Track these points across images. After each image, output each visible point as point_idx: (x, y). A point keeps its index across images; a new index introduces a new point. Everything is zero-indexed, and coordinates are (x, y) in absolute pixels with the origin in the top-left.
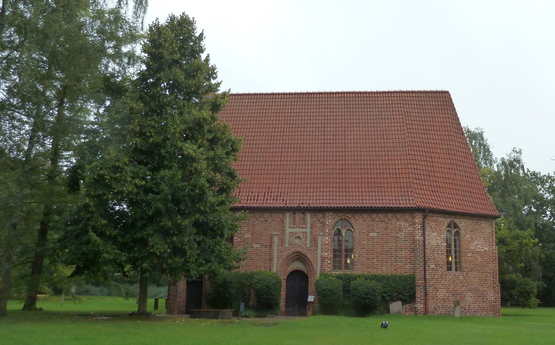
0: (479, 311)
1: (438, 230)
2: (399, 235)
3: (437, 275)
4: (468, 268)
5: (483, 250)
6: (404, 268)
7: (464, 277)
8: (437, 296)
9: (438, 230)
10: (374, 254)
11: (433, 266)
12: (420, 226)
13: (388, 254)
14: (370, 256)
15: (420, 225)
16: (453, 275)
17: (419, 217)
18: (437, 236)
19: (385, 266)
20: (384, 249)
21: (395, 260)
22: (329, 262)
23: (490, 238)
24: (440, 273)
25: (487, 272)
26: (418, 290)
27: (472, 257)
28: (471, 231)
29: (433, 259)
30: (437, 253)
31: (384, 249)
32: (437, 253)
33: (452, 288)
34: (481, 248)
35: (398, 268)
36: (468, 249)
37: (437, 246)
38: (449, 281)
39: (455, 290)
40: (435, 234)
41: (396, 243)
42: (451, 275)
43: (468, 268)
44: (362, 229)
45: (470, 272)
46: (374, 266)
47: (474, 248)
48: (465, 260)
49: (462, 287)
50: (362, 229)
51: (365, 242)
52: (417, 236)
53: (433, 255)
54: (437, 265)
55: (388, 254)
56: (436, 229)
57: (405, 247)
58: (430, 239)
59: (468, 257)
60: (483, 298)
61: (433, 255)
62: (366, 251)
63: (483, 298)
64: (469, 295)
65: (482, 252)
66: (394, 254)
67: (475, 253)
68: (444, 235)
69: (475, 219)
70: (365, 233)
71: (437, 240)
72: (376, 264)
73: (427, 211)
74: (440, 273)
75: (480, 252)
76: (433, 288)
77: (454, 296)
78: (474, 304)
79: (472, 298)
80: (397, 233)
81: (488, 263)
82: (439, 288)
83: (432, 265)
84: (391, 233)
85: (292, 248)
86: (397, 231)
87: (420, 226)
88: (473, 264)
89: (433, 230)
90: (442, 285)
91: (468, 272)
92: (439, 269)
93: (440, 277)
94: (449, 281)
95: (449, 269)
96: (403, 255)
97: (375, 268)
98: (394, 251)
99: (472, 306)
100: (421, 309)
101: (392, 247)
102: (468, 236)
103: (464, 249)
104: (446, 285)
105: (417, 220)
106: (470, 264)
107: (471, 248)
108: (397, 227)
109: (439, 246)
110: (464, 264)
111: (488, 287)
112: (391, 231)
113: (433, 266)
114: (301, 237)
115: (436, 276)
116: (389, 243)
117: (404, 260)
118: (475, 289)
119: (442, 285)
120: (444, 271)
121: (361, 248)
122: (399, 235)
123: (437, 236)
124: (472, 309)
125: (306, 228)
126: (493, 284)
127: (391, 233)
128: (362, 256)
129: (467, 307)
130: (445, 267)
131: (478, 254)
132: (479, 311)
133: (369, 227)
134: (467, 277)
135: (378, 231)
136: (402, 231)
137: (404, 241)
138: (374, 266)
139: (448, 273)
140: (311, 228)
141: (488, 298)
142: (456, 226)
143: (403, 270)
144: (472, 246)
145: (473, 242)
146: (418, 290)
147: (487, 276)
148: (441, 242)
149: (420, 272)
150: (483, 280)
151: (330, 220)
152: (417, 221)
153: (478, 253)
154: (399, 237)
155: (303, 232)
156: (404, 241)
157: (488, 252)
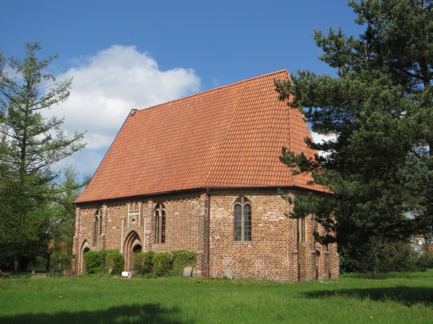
0: (271, 276)
1: (225, 206)
2: (193, 212)
3: (222, 244)
4: (259, 237)
5: (277, 220)
6: (195, 240)
7: (254, 246)
8: (222, 263)
9: (225, 206)
10: (177, 230)
11: (219, 237)
12: (204, 203)
13: (185, 229)
14: (175, 231)
15: (204, 202)
16: (241, 244)
17: (204, 196)
18: (224, 211)
19: (183, 239)
20: (183, 224)
21: (190, 234)
22: (148, 238)
23: (288, 208)
24: (225, 243)
25: (281, 240)
26: (198, 258)
27: (265, 227)
28: (264, 203)
29: (218, 231)
30: (223, 226)
31: (183, 224)
32: (223, 226)
33: (239, 256)
34: (277, 218)
35: (191, 240)
36: (260, 220)
37: (223, 219)
38: (235, 249)
39: (242, 258)
40: (222, 209)
41: (190, 219)
42: (239, 244)
43: (259, 237)
44: (170, 209)
45: (260, 241)
46: (177, 240)
47: (267, 218)
48: (254, 230)
49: (250, 254)
50: (170, 209)
51: (171, 220)
52: (202, 212)
53: (219, 228)
54: (222, 236)
55: (185, 229)
56: (223, 204)
57: (196, 222)
58: (215, 214)
59: (260, 227)
60: (276, 265)
61: (219, 228)
62: (172, 227)
63: (276, 265)
64: (259, 261)
65: (277, 222)
66: (189, 229)
67: (268, 223)
68: (231, 209)
69: (268, 191)
70: (172, 212)
71: (224, 214)
72: (178, 238)
73: (208, 190)
74: (225, 243)
75: (273, 222)
76: (217, 256)
77: (241, 263)
78: (264, 270)
79: (263, 265)
80: (191, 211)
81: (284, 232)
82: (224, 256)
83: (217, 236)
84: (187, 211)
85: (130, 228)
86: (191, 209)
87: (204, 203)
88: (265, 234)
89: (219, 206)
90: (227, 253)
91: (258, 240)
92: (225, 239)
93: (225, 246)
94: (235, 249)
95: (237, 238)
96: (194, 229)
97: (178, 241)
98: (189, 226)
99: (262, 272)
100: (199, 275)
101: (188, 222)
102: (260, 208)
103: (254, 220)
104: (232, 253)
105: (202, 199)
106: (261, 234)
107: (263, 218)
108: (191, 206)
109: (226, 219)
110: (253, 234)
111: (283, 254)
112: (188, 209)
113: (219, 237)
114: (135, 219)
115: (221, 246)
116: (186, 219)
117: (195, 234)
118: (266, 256)
119: (227, 253)
120: (230, 241)
121: (170, 225)
122: (193, 212)
123: (224, 211)
124: (262, 275)
125: (138, 212)
126: (289, 251)
127: (187, 211)
128: (170, 232)
129: (256, 273)
130: (231, 238)
131: (272, 223)
132: (271, 276)
133: (174, 207)
134: (257, 246)
135: (180, 210)
136: (194, 209)
137: (195, 217)
138: (177, 240)
139: (235, 243)
140: (141, 212)
141: (282, 265)
142: (246, 200)
143: (194, 242)
144: (265, 217)
145: (266, 213)
146: (198, 258)
147: (283, 244)
148: (229, 216)
149: (201, 243)
150: (277, 247)
151: (151, 204)
152: (202, 200)
153: (271, 223)
154: (192, 214)
155: (136, 215)
156: (195, 217)
157: (284, 222)
